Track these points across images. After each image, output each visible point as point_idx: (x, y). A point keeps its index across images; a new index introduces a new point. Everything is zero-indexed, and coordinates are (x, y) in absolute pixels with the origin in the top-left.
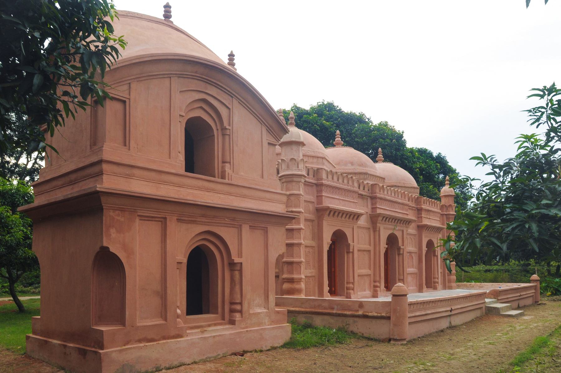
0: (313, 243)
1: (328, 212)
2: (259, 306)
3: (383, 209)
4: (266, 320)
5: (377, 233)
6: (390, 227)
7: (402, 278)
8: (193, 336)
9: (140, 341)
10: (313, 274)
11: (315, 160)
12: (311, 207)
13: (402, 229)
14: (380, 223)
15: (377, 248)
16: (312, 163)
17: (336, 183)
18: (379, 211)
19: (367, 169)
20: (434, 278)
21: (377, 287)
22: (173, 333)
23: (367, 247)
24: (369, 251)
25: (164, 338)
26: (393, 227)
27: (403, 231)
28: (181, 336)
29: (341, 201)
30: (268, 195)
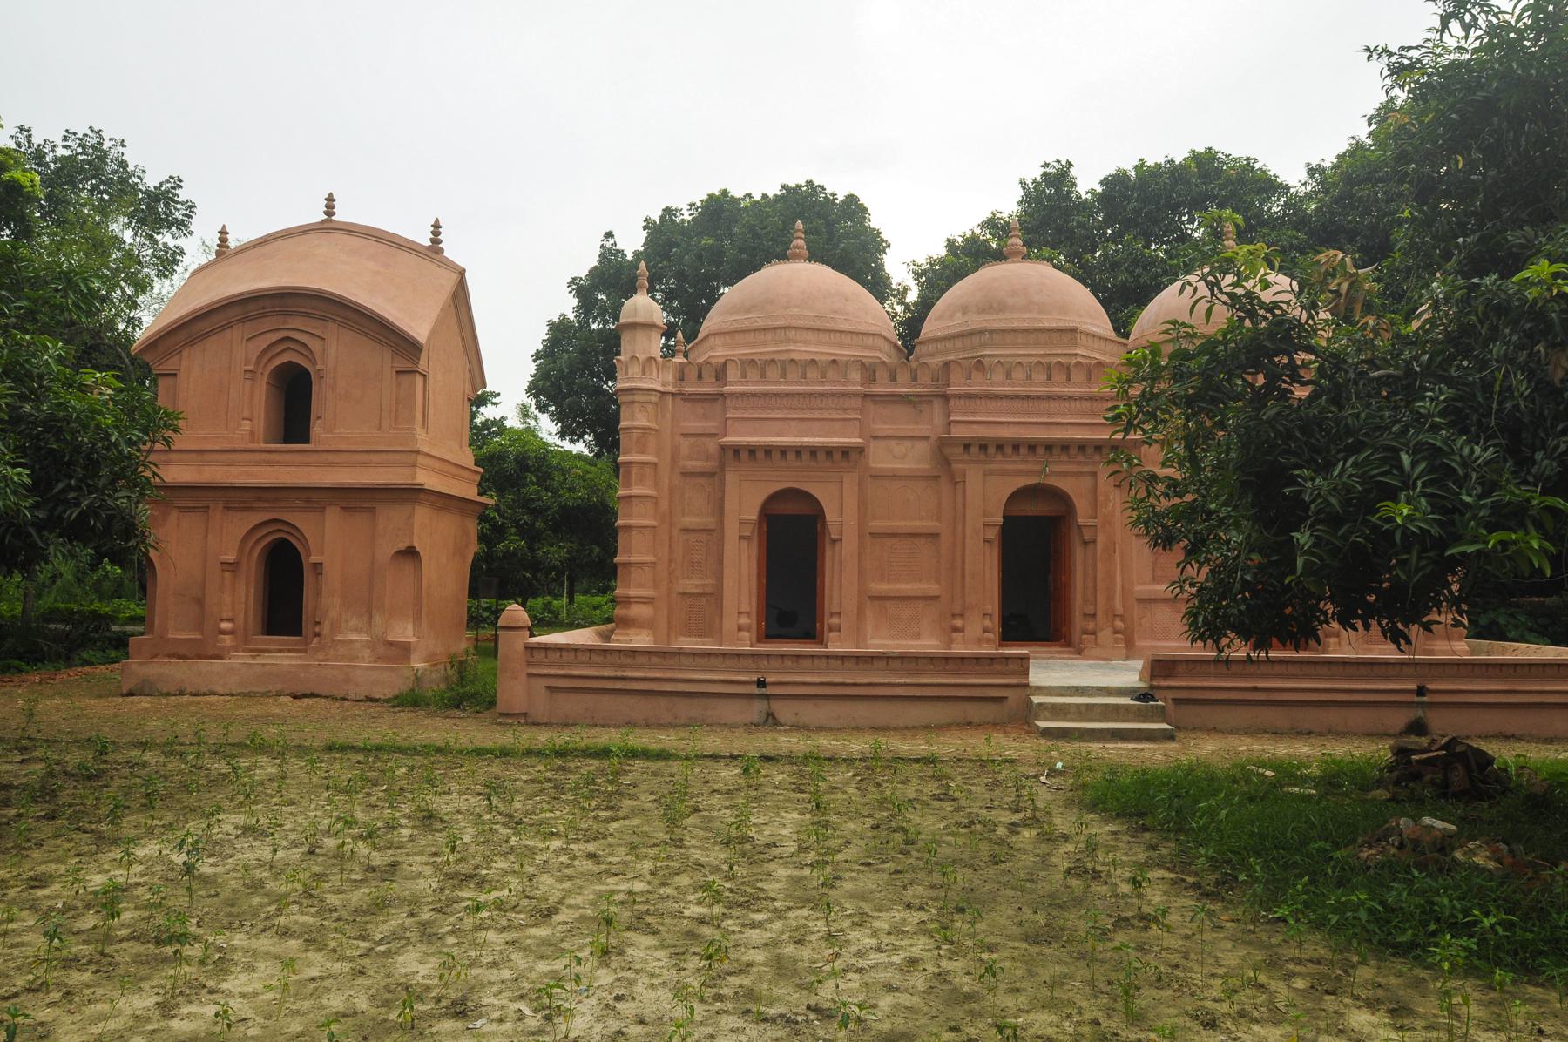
0: (710, 522)
1: (730, 453)
2: (358, 630)
3: (974, 424)
4: (367, 653)
5: (959, 486)
6: (1022, 467)
7: (1090, 609)
8: (239, 659)
9: (169, 656)
10: (708, 590)
11: (769, 336)
12: (712, 446)
13: (1086, 469)
14: (960, 462)
15: (960, 528)
16: (764, 344)
17: (797, 383)
18: (958, 432)
19: (1001, 316)
21: (955, 629)
22: (210, 653)
23: (928, 525)
24: (934, 536)
25: (199, 657)
26: (1037, 468)
27: (1094, 474)
28: (221, 658)
29: (793, 424)
30: (375, 458)
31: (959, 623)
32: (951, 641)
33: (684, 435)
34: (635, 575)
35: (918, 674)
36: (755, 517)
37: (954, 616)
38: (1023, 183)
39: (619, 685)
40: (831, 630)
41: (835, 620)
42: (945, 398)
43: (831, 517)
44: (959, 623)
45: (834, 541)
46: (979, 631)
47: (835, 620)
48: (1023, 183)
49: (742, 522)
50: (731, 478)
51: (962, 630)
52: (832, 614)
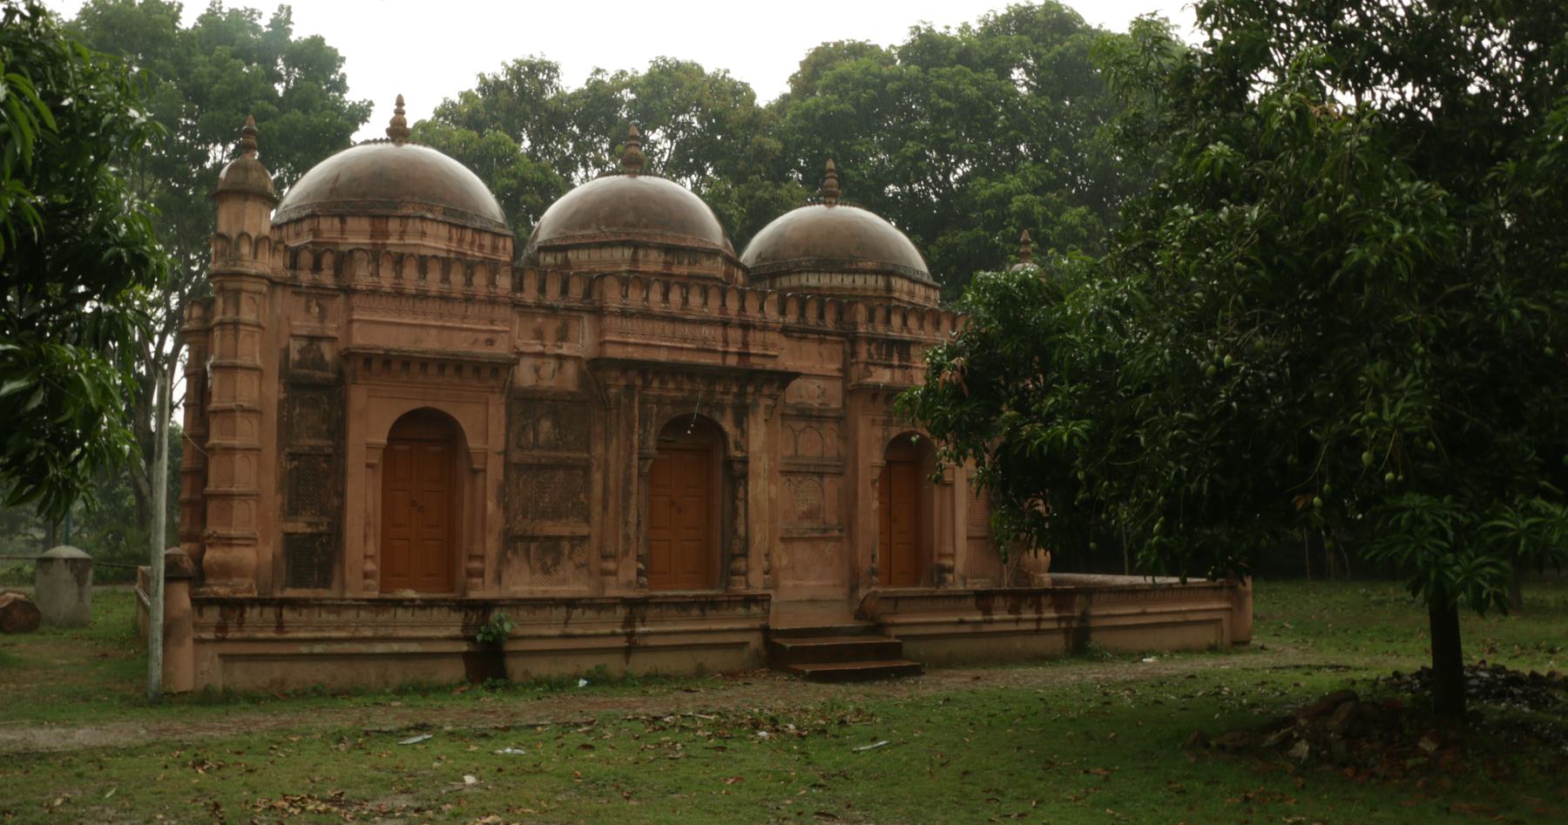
1: (360, 364)
20: (941, 556)
31: (611, 565)
32: (603, 586)
33: (293, 336)
34: (239, 510)
35: (662, 621)
36: (385, 441)
37: (605, 557)
38: (481, 76)
39: (318, 649)
40: (471, 574)
41: (476, 564)
42: (599, 312)
43: (474, 444)
44: (611, 565)
45: (475, 472)
46: (633, 575)
47: (476, 564)
48: (481, 76)
49: (370, 447)
50: (358, 397)
51: (614, 573)
52: (471, 557)
